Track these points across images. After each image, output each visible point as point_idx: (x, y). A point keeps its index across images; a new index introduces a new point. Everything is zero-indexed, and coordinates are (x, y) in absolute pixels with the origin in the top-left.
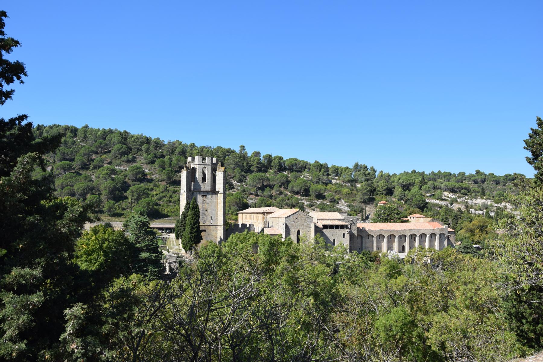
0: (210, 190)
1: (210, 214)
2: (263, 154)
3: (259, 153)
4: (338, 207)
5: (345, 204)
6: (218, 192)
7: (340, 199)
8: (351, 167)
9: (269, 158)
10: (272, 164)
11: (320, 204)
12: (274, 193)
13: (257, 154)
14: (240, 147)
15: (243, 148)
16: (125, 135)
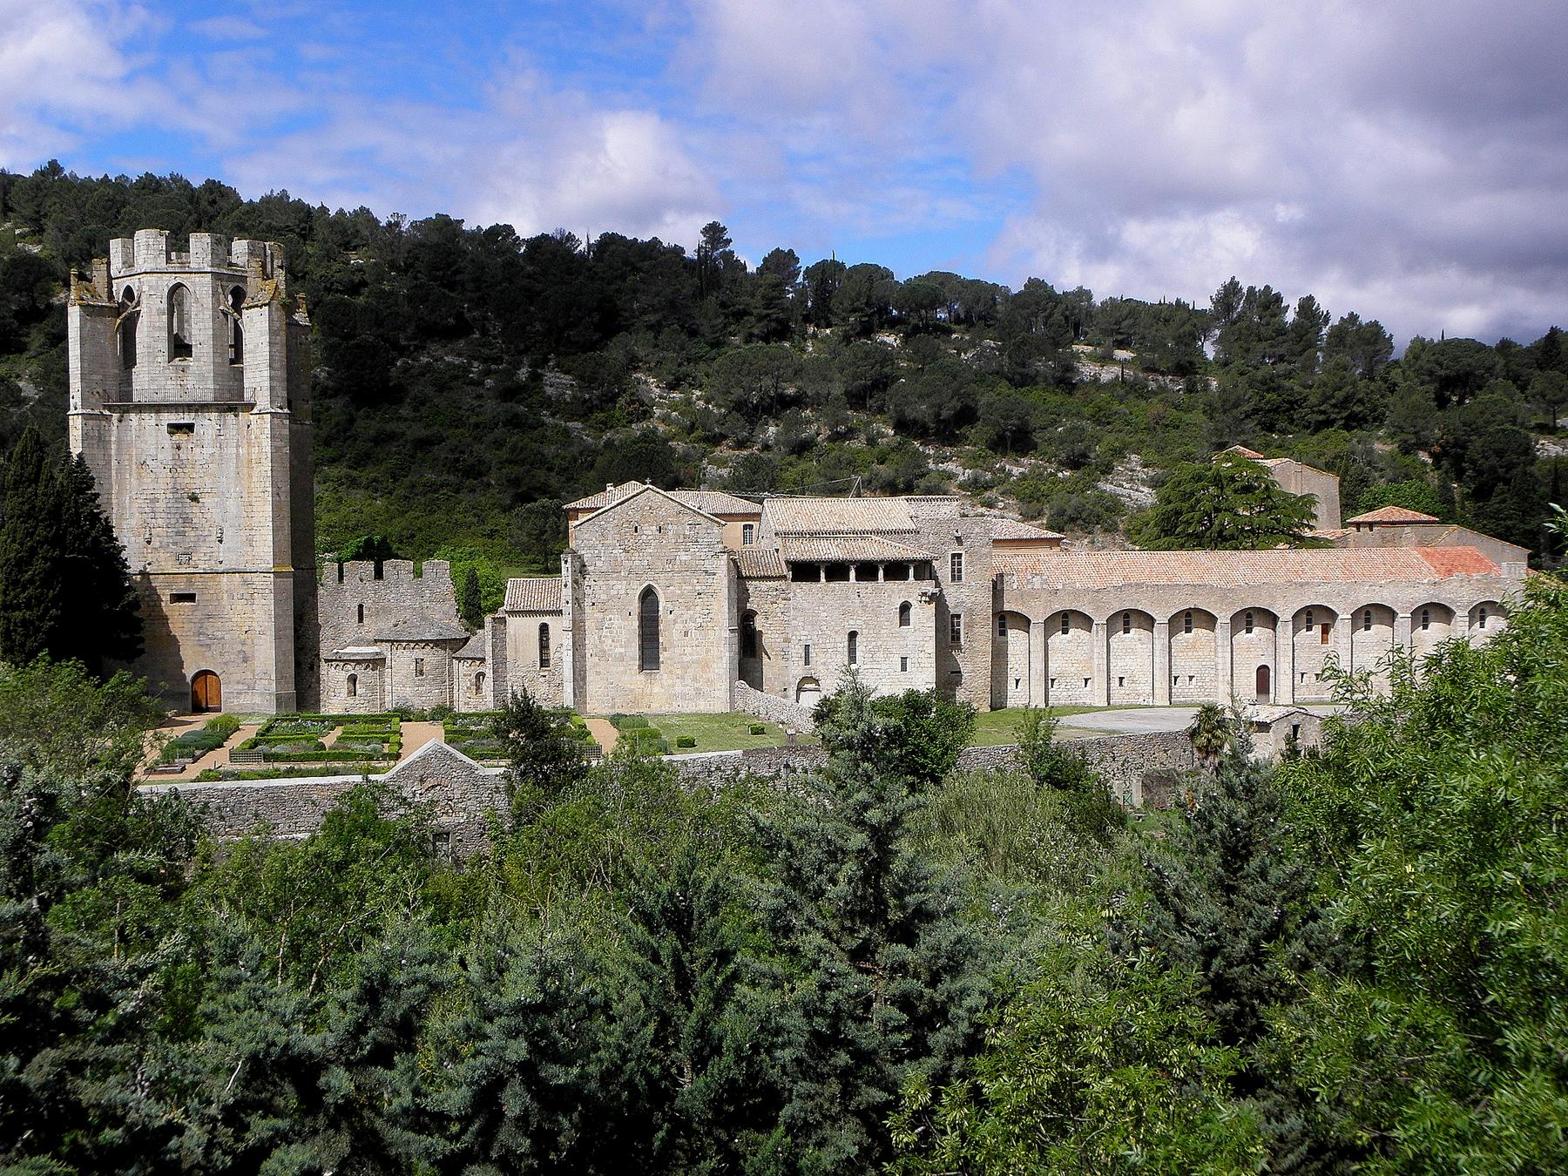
0: (209, 398)
1: (215, 515)
2: (806, 261)
3: (791, 257)
4: (1109, 487)
5: (1142, 473)
6: (253, 406)
7: (1119, 453)
8: (1204, 304)
9: (826, 272)
10: (833, 303)
11: (1023, 477)
12: (816, 428)
13: (781, 262)
14: (705, 231)
15: (714, 233)
16: (214, 202)
